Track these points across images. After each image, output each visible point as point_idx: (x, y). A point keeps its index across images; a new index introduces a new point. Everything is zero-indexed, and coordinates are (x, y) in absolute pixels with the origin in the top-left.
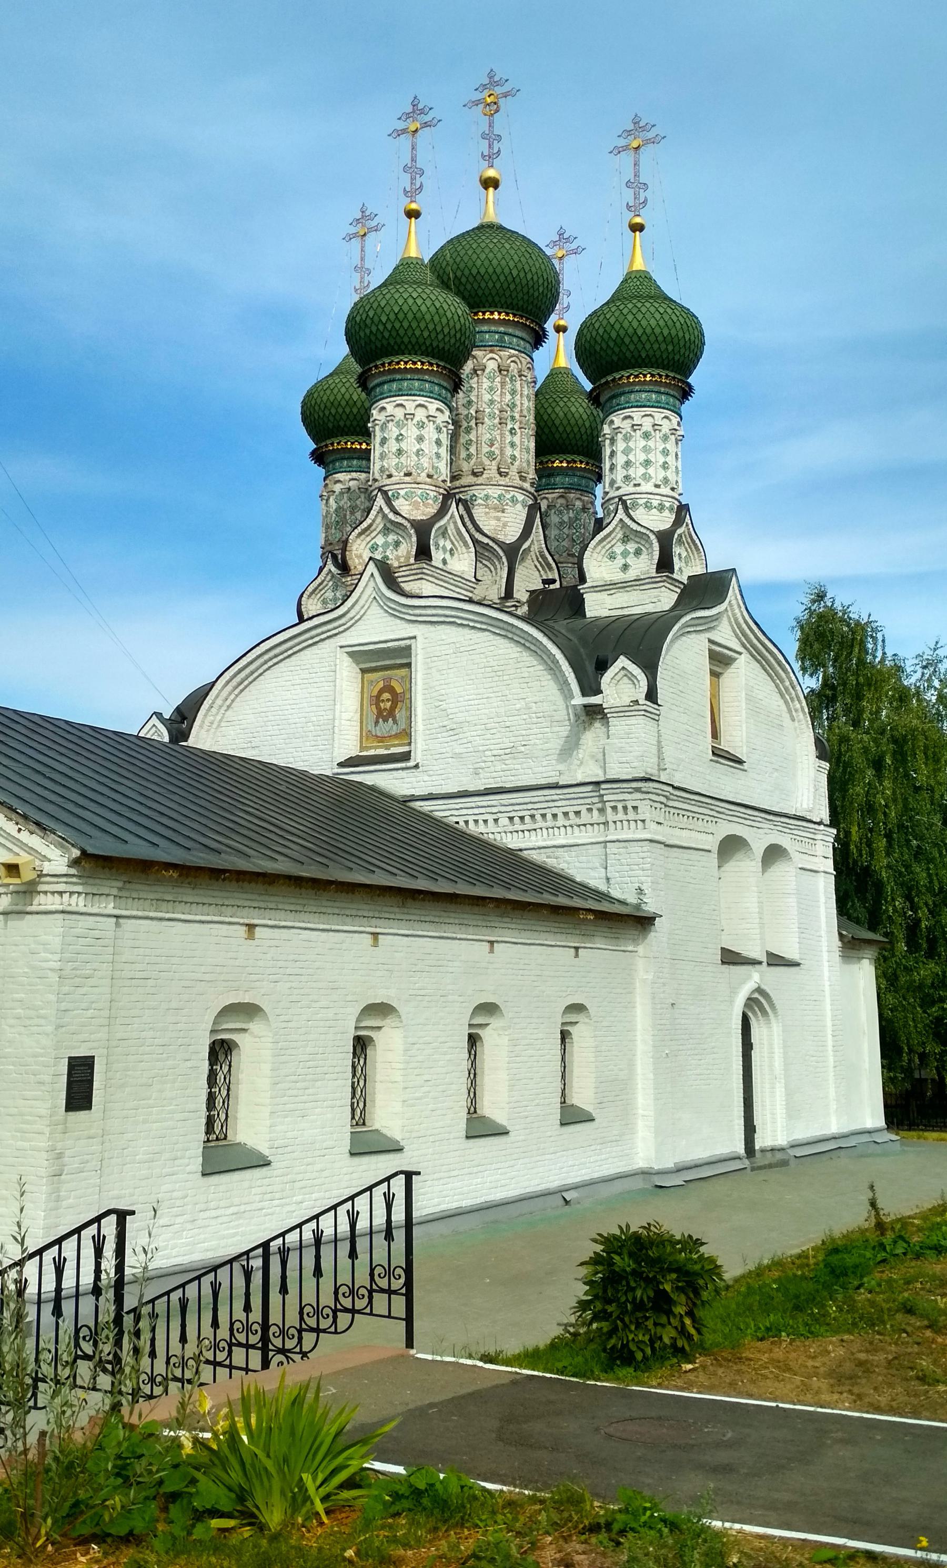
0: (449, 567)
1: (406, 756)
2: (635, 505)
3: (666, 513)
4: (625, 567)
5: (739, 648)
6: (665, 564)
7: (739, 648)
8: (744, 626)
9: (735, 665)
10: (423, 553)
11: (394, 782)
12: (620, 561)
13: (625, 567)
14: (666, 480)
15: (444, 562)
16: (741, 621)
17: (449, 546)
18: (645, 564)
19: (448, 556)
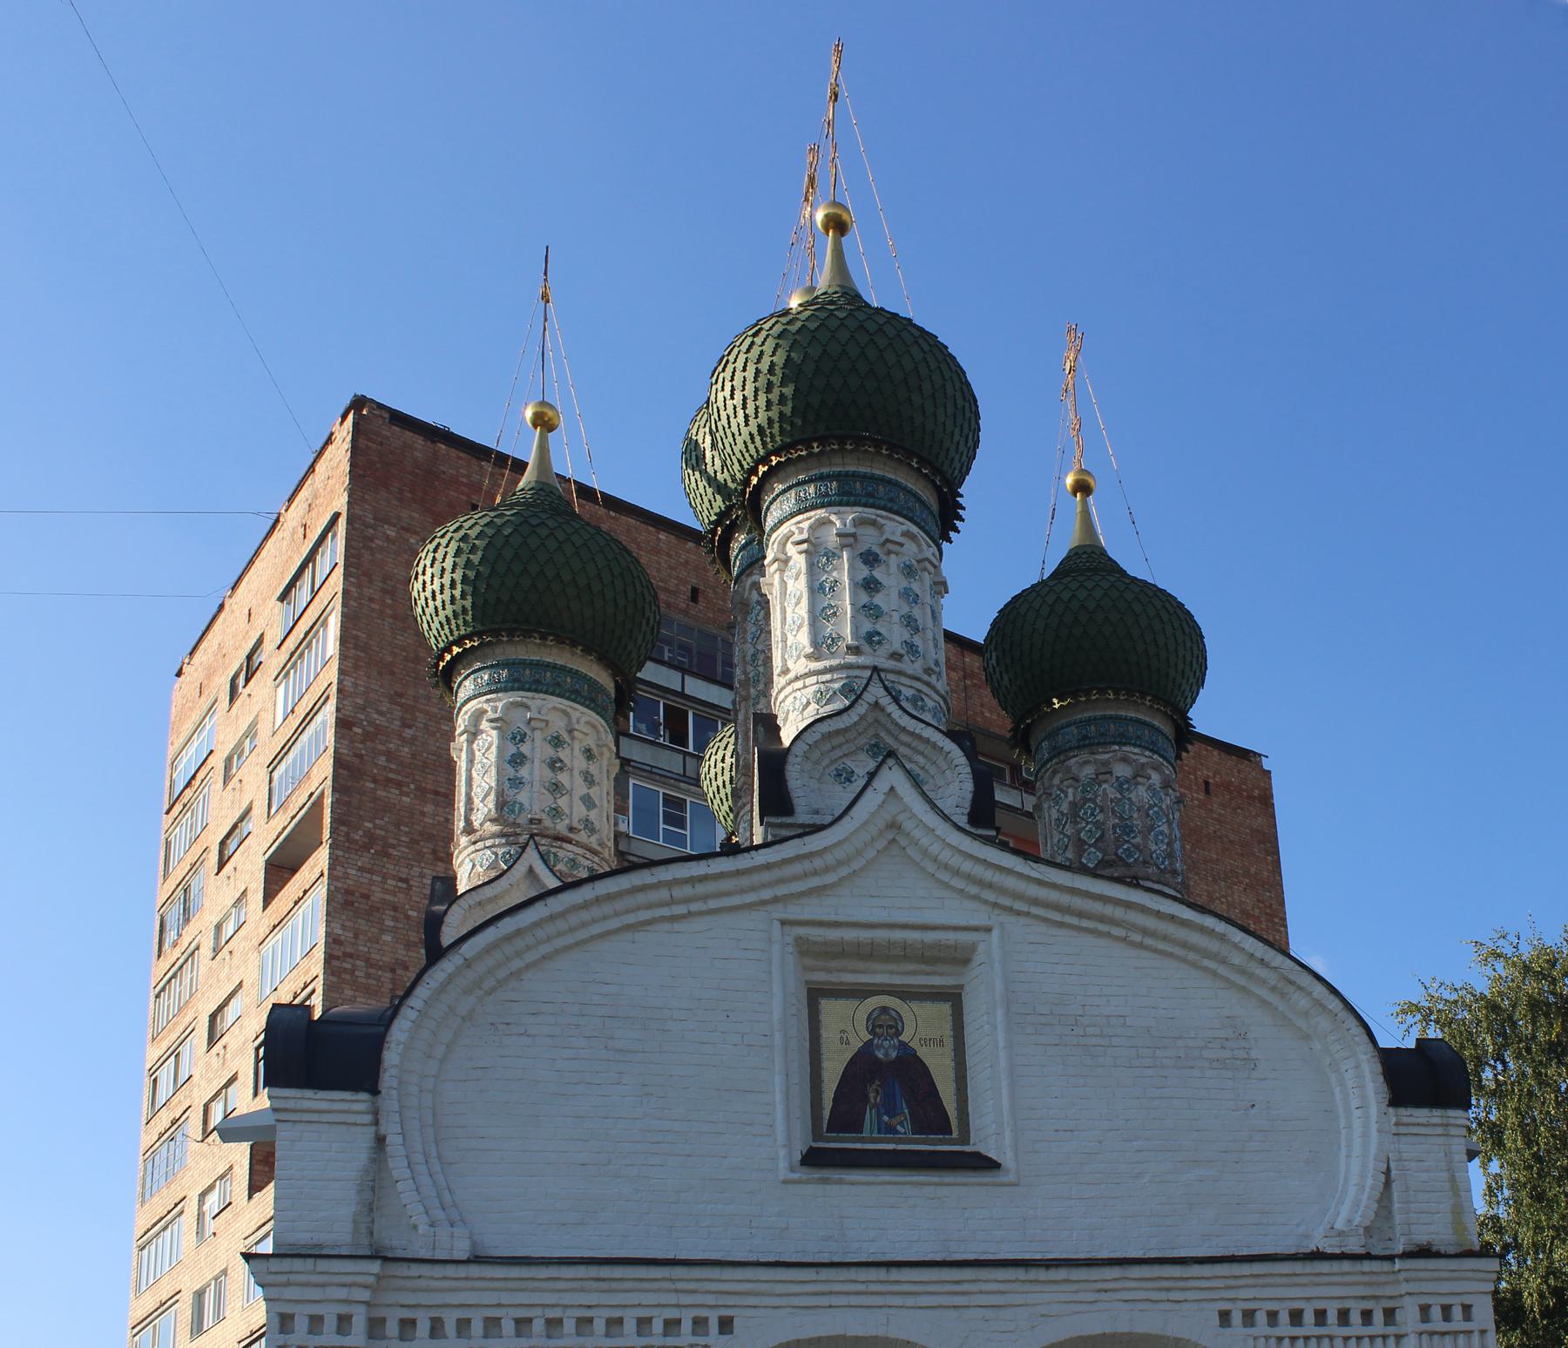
7: (980, 917)
8: (967, 866)
9: (978, 958)
16: (956, 861)
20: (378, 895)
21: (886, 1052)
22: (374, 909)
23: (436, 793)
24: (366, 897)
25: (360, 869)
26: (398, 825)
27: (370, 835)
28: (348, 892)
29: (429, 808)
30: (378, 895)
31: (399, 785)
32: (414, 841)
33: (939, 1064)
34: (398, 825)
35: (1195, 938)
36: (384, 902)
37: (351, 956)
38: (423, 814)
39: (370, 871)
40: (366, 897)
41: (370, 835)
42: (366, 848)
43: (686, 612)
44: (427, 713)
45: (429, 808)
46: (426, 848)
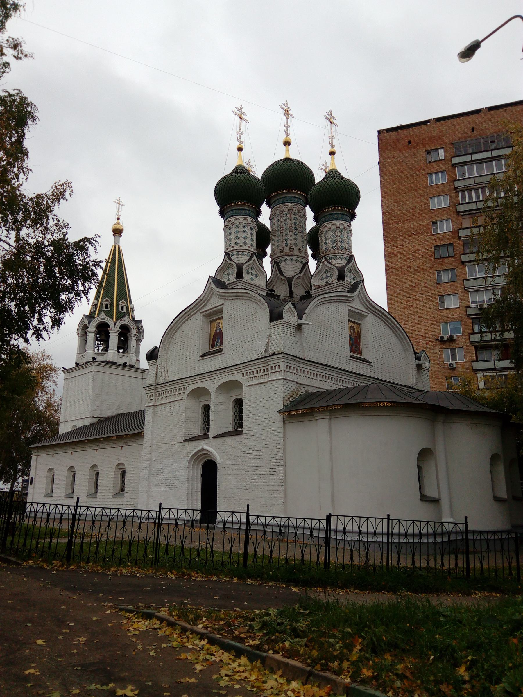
20: (396, 251)
23: (407, 220)
24: (393, 253)
25: (391, 247)
26: (399, 232)
28: (389, 253)
29: (406, 225)
30: (396, 251)
31: (398, 222)
32: (403, 234)
34: (399, 232)
36: (397, 252)
37: (391, 268)
38: (404, 227)
39: (394, 246)
40: (393, 253)
41: (393, 238)
42: (392, 241)
44: (403, 201)
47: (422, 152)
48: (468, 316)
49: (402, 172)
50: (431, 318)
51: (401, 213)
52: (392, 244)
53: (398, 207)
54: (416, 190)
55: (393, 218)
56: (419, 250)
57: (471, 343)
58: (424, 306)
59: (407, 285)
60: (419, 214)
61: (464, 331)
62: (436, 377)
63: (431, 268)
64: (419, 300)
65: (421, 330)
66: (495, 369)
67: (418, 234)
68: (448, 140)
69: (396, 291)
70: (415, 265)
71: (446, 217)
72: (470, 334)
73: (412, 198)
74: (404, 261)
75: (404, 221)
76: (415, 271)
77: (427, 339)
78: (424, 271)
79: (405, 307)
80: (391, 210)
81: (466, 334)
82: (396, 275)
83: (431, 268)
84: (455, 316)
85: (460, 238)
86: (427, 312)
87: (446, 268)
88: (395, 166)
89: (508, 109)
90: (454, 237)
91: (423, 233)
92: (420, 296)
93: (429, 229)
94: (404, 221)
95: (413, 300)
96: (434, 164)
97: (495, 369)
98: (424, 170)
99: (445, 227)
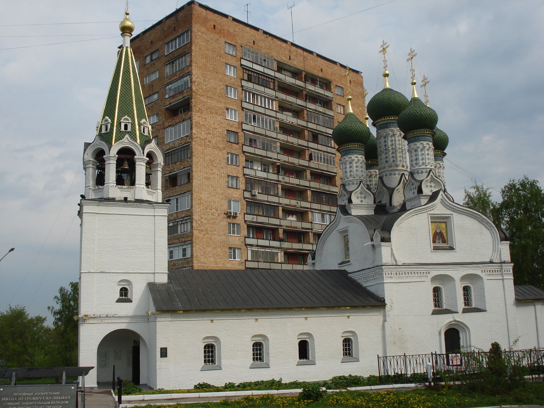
0: (363, 203)
1: (349, 261)
2: (414, 173)
3: (424, 174)
4: (414, 193)
5: (451, 213)
6: (420, 191)
10: (350, 201)
11: (348, 268)
12: (413, 191)
13: (414, 193)
14: (423, 163)
15: (362, 201)
17: (363, 196)
18: (416, 191)
19: (363, 199)
21: (438, 231)
22: (200, 126)
27: (199, 109)
30: (201, 123)
32: (207, 109)
33: (444, 232)
35: (477, 216)
37: (197, 137)
41: (199, 109)
42: (198, 112)
43: (252, 47)
45: (209, 101)
46: (209, 110)
47: (222, 40)
48: (245, 198)
49: (208, 50)
50: (222, 194)
51: (206, 88)
52: (199, 114)
53: (204, 81)
54: (217, 73)
55: (201, 90)
56: (216, 129)
57: (245, 221)
58: (218, 181)
59: (208, 157)
60: (218, 96)
61: (241, 210)
62: (223, 246)
63: (224, 148)
64: (215, 174)
65: (214, 202)
66: (257, 246)
67: (216, 113)
68: (239, 42)
69: (200, 161)
70: (214, 141)
71: (235, 108)
72: (245, 214)
73: (215, 79)
74: (207, 134)
75: (207, 97)
76: (214, 147)
77: (219, 212)
78: (220, 149)
79: (206, 178)
80: (200, 82)
81: (243, 214)
82: (201, 146)
83: (224, 148)
84: (237, 196)
85: (243, 130)
86: (220, 187)
87: (233, 152)
88: (203, 42)
89: (274, 39)
90: (239, 128)
91: (220, 115)
92: (215, 170)
93: (224, 113)
94: (207, 97)
95: (211, 173)
96: (230, 57)
97: (257, 246)
98: (223, 58)
99: (233, 117)
